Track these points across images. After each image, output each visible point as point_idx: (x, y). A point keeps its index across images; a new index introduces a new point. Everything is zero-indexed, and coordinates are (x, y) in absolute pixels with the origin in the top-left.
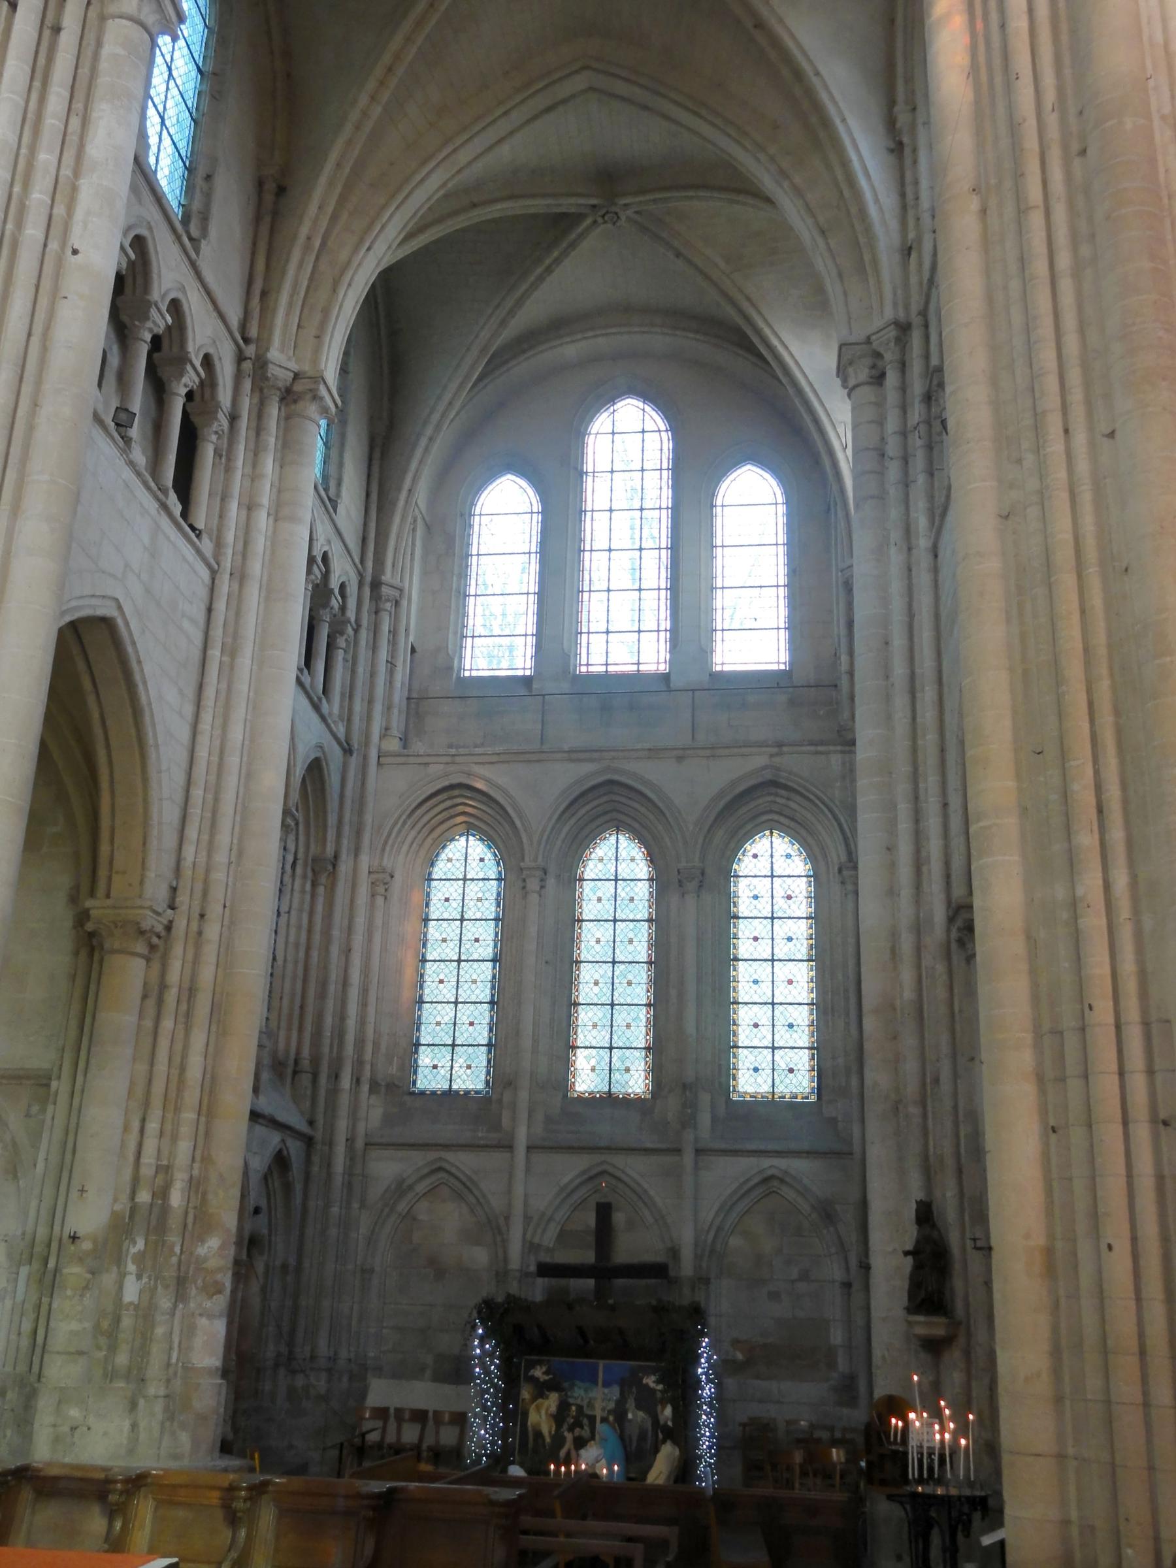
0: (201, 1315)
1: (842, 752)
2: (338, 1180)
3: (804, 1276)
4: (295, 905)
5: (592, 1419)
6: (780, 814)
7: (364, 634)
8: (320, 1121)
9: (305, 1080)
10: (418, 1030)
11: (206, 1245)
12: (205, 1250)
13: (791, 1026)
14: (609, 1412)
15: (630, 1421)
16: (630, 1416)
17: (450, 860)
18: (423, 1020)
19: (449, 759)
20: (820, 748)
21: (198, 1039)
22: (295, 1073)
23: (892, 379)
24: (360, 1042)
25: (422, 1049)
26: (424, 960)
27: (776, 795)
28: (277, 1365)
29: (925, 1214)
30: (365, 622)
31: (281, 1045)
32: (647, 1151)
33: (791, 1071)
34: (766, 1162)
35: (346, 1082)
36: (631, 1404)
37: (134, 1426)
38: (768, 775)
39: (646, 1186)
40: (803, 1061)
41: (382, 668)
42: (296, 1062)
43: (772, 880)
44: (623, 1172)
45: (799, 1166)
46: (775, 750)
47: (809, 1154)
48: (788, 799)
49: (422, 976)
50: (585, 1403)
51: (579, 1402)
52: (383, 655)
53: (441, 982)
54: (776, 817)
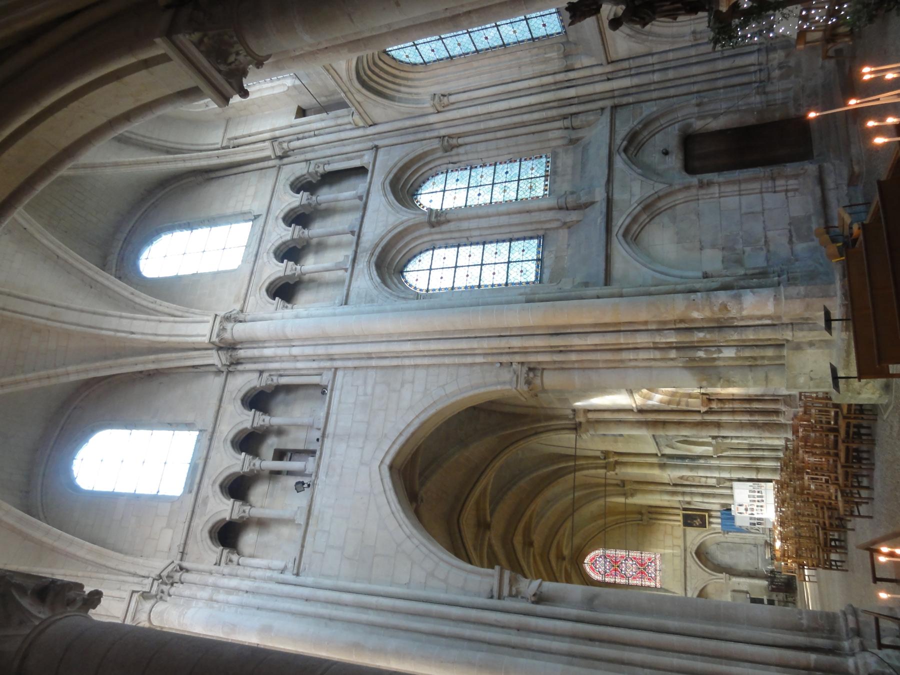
2: (636, 81)
4: (475, 156)
7: (309, 156)
8: (601, 104)
9: (577, 122)
10: (523, 41)
17: (407, 56)
18: (516, 40)
19: (349, 95)
21: (576, 341)
22: (573, 129)
24: (543, 89)
25: (535, 36)
26: (477, 51)
28: (765, 93)
30: (302, 157)
31: (560, 142)
35: (572, 92)
37: (811, 344)
41: (320, 139)
42: (566, 128)
49: (487, 49)
52: (313, 141)
53: (486, 38)
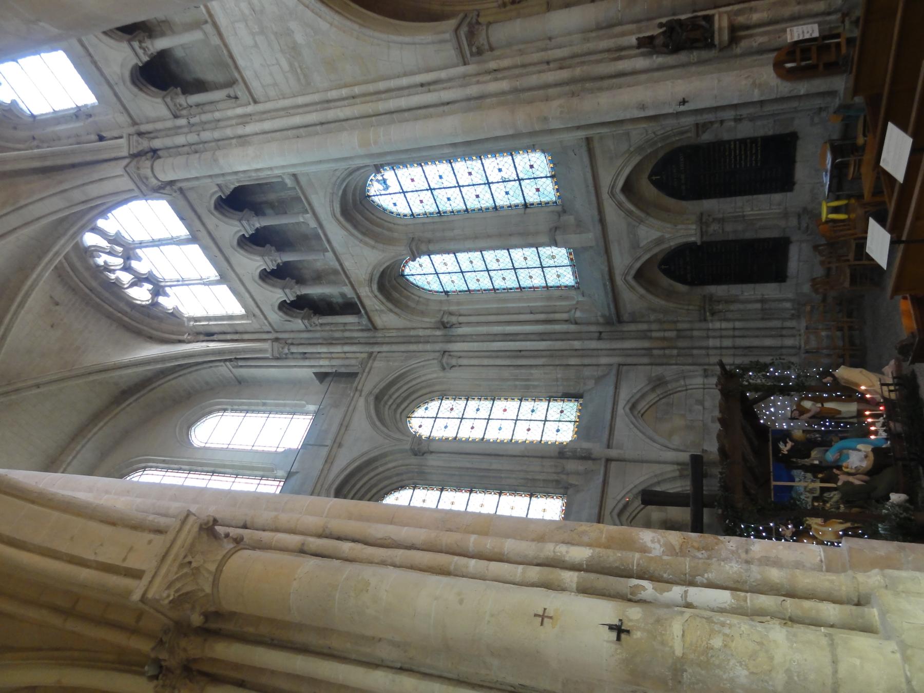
0: (747, 552)
1: (374, 360)
3: (701, 402)
5: (823, 490)
6: (399, 406)
11: (649, 544)
12: (657, 546)
13: (533, 411)
14: (815, 477)
15: (820, 462)
16: (816, 462)
20: (367, 370)
23: (156, 144)
27: (386, 403)
29: (647, 44)
32: (605, 483)
33: (562, 412)
34: (620, 410)
36: (807, 462)
38: (372, 399)
39: (631, 486)
40: (556, 406)
43: (437, 420)
44: (619, 502)
45: (625, 395)
46: (357, 394)
47: (617, 387)
48: (390, 397)
50: (811, 496)
51: (809, 500)
54: (400, 411)
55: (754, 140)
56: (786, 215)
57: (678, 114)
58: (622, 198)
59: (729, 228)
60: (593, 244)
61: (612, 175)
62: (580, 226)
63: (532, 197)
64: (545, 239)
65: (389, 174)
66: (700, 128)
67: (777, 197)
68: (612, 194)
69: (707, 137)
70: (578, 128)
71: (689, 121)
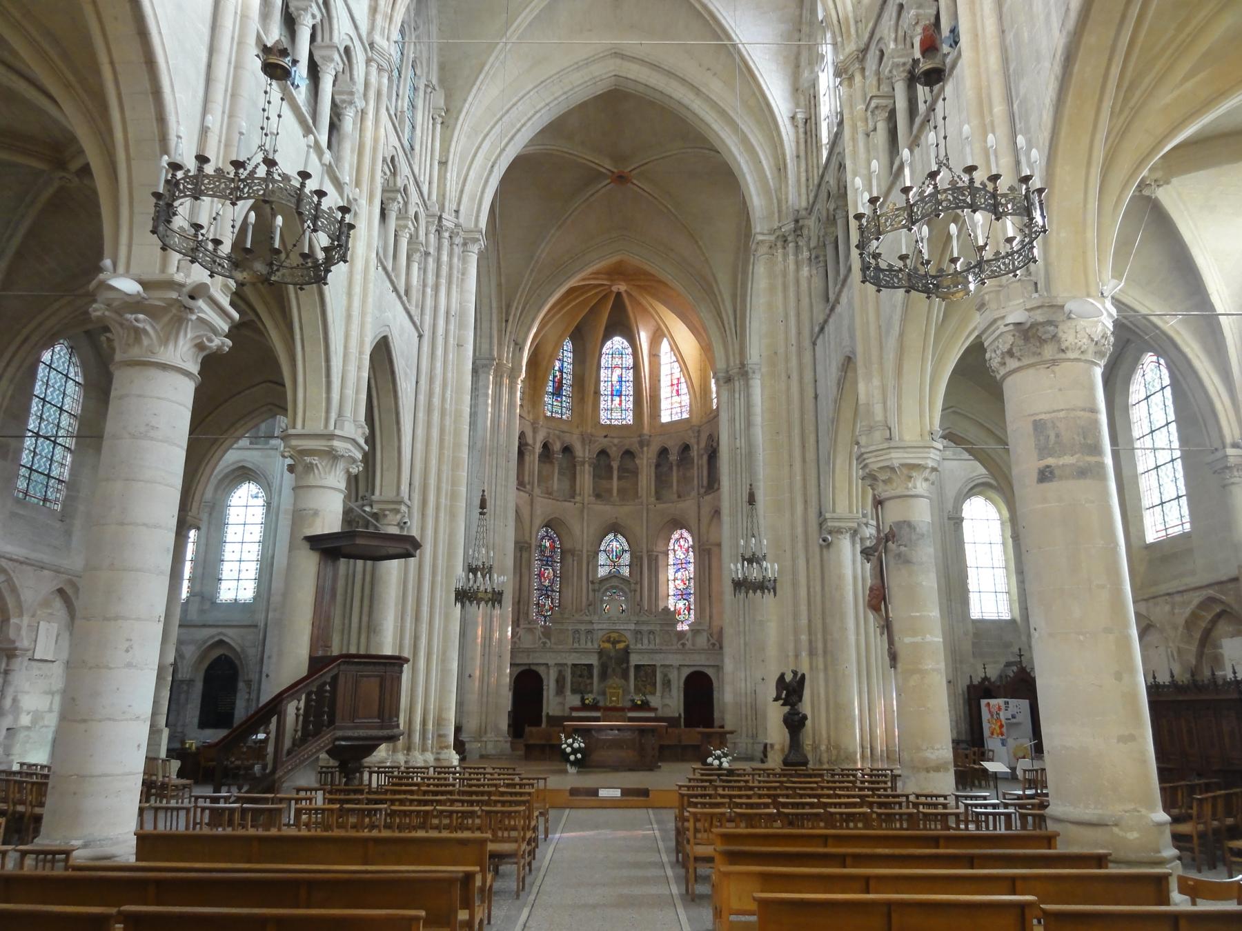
55: (233, 709)
56: (184, 726)
57: (261, 672)
58: (216, 639)
59: (183, 696)
60: (189, 618)
61: (231, 636)
62: (202, 611)
63: (224, 585)
64: (197, 589)
65: (261, 502)
66: (249, 683)
67: (196, 720)
68: (220, 634)
69: (241, 685)
70: (266, 625)
71: (254, 677)
